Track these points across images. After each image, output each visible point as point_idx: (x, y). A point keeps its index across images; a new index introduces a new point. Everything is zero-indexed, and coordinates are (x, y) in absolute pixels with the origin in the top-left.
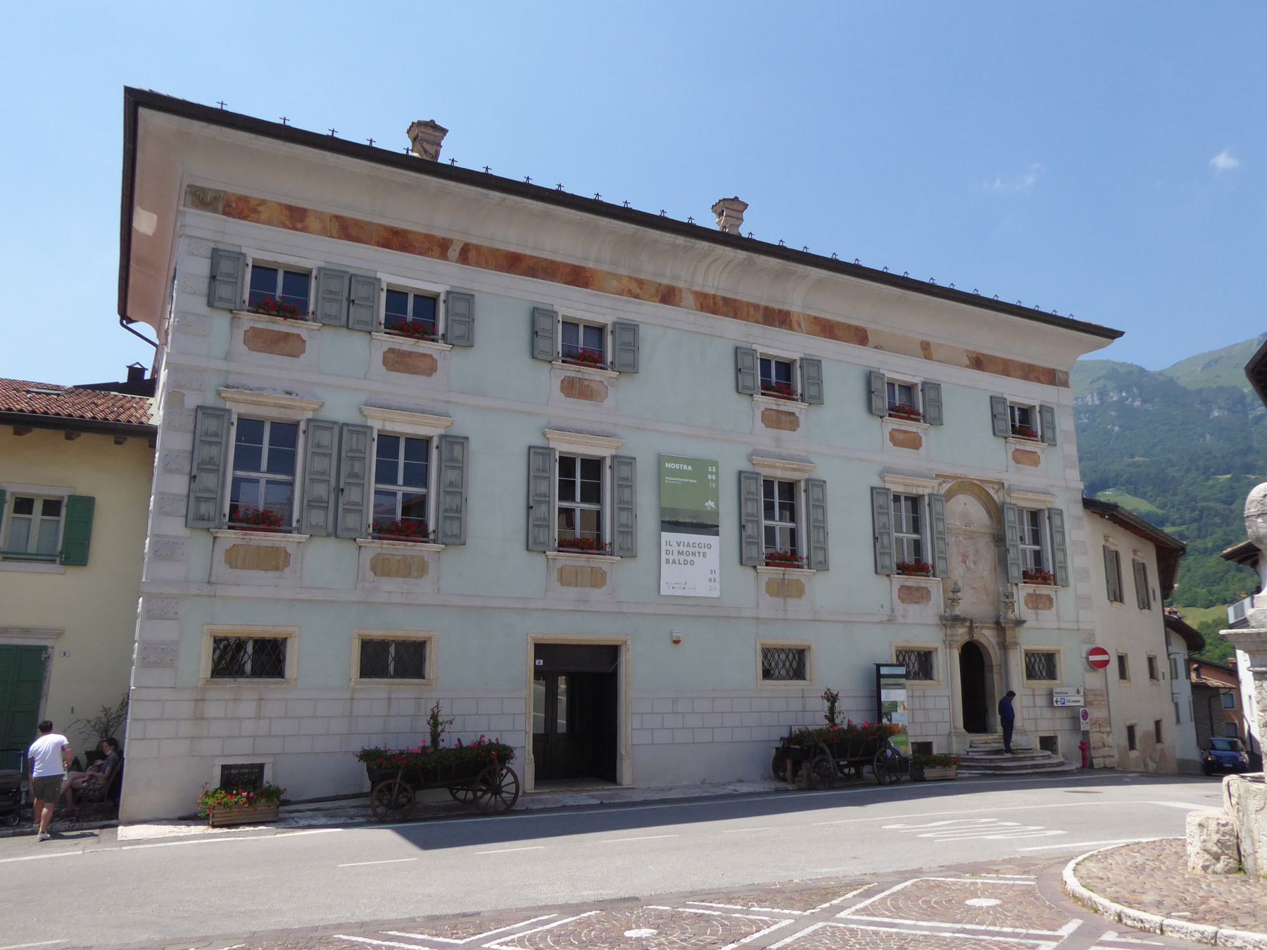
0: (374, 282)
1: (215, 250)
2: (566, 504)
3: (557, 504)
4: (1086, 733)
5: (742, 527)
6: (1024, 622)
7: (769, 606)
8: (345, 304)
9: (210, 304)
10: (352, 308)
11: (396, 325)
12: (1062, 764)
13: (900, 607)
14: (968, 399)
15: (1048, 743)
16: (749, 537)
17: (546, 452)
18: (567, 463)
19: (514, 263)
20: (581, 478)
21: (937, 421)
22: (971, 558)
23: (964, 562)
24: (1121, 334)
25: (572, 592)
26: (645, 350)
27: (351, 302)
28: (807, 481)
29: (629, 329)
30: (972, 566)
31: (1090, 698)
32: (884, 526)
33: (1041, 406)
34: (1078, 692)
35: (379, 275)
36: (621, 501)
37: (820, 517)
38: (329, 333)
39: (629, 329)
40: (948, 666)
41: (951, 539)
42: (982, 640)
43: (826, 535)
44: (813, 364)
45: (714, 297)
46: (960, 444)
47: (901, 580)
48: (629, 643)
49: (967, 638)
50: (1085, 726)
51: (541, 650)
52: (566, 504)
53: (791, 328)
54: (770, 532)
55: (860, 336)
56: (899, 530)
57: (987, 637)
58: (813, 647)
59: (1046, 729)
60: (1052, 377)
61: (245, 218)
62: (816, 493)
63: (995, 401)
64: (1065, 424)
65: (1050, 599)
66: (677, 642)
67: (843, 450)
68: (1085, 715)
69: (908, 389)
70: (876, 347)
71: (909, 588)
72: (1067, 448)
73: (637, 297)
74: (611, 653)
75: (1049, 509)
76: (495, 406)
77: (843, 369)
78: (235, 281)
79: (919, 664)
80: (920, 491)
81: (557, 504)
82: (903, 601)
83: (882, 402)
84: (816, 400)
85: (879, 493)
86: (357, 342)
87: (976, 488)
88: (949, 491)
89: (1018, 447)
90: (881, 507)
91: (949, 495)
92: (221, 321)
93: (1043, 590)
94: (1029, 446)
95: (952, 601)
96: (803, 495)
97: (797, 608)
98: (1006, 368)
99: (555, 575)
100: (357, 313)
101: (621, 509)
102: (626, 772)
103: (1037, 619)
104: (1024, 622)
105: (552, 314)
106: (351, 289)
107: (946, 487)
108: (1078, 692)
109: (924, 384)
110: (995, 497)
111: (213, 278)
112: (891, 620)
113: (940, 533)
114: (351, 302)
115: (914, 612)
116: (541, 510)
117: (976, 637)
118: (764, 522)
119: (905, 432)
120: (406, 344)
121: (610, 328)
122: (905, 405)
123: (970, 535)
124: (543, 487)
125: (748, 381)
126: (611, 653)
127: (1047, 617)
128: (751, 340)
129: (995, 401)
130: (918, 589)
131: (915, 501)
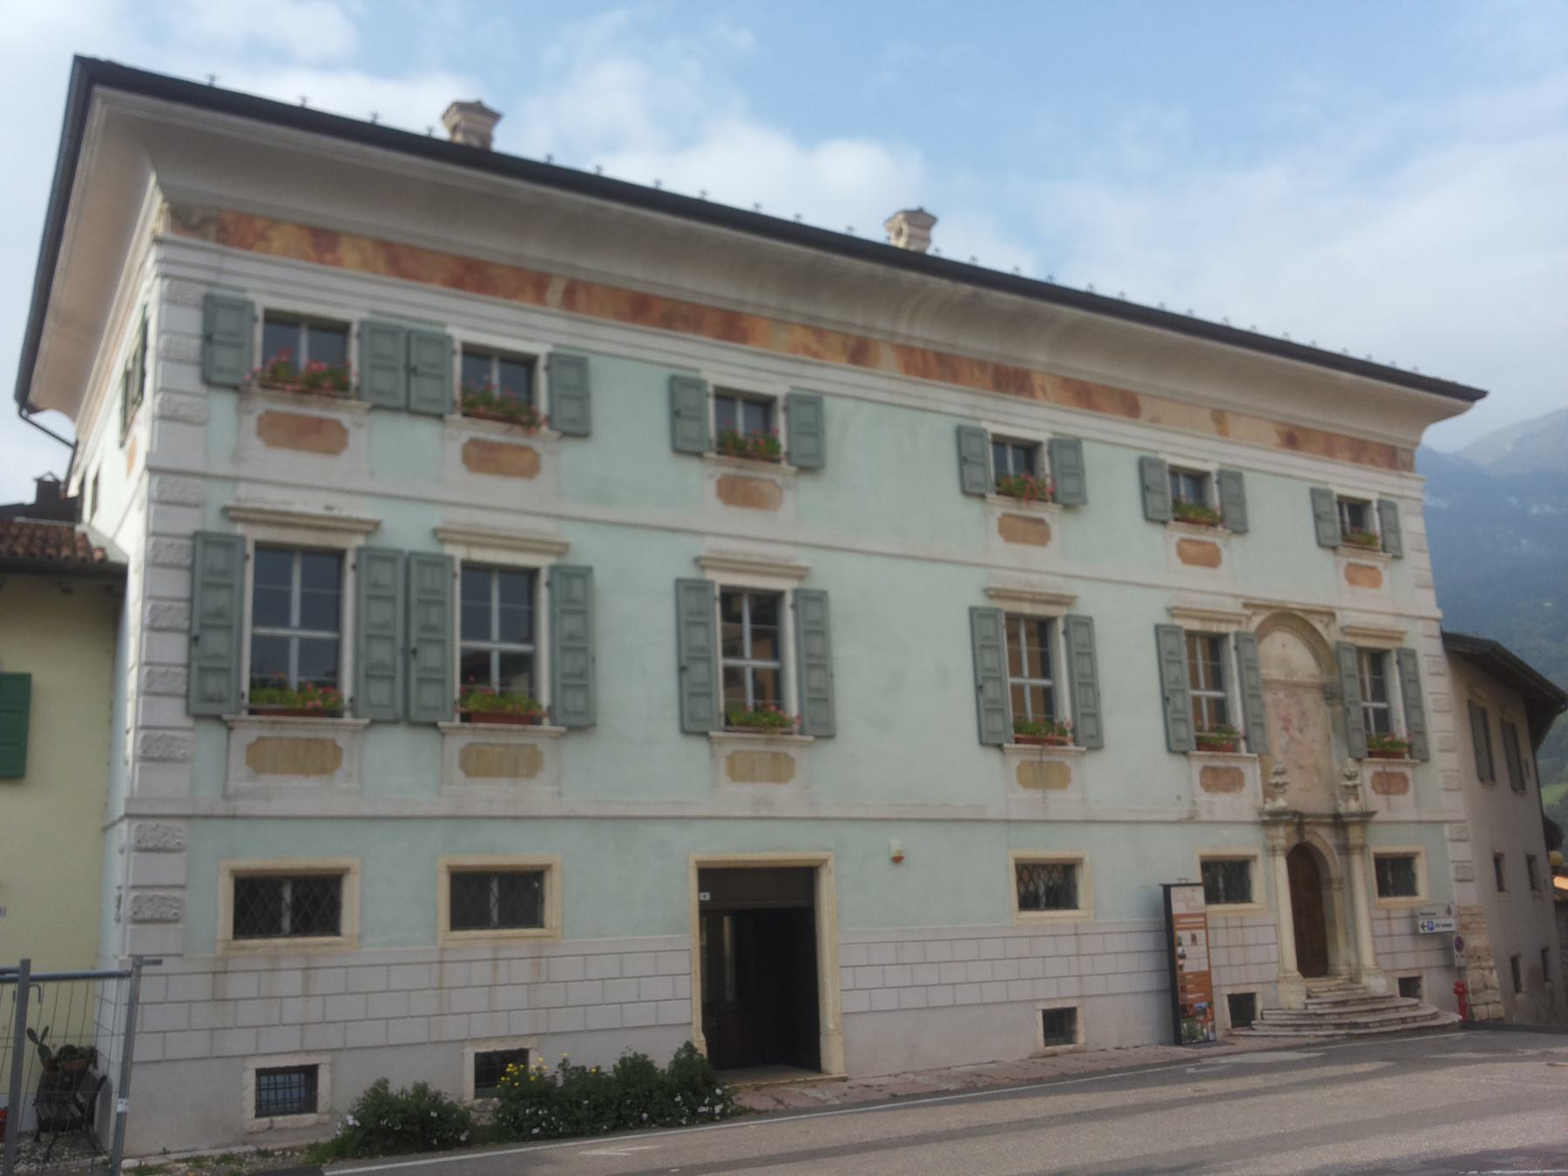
0: (443, 341)
1: (208, 299)
2: (732, 662)
3: (721, 662)
4: (1461, 970)
5: (979, 689)
6: (1373, 813)
7: (1024, 802)
8: (402, 374)
9: (207, 382)
10: (414, 382)
11: (475, 406)
12: (1435, 1016)
13: (1204, 798)
14: (1282, 492)
15: (1409, 986)
16: (990, 701)
17: (701, 587)
18: (730, 597)
19: (641, 309)
20: (753, 616)
21: (1240, 529)
22: (1296, 722)
23: (1286, 729)
24: (1472, 395)
25: (749, 790)
26: (832, 432)
27: (411, 371)
28: (1067, 618)
29: (809, 404)
30: (1298, 736)
31: (1466, 919)
32: (1177, 682)
33: (1380, 502)
34: (1449, 911)
35: (450, 330)
36: (810, 655)
37: (1088, 671)
38: (382, 421)
39: (809, 404)
40: (1272, 883)
41: (1268, 697)
42: (1316, 842)
43: (1097, 695)
44: (1070, 446)
45: (924, 352)
46: (1277, 557)
47: (1200, 760)
48: (831, 862)
49: (1295, 841)
50: (1459, 961)
51: (710, 876)
52: (732, 662)
53: (1032, 394)
54: (1017, 691)
55: (1129, 405)
56: (1195, 685)
57: (1324, 839)
58: (1087, 860)
59: (1408, 964)
60: (1394, 458)
61: (249, 247)
62: (1080, 635)
63: (1318, 495)
64: (1412, 526)
65: (1404, 779)
66: (897, 860)
67: (1119, 576)
68: (1460, 944)
69: (1198, 479)
70: (1152, 421)
71: (1214, 770)
72: (1417, 561)
73: (816, 355)
74: (804, 877)
75: (1399, 651)
76: (629, 518)
77: (1112, 454)
78: (239, 342)
79: (1226, 879)
80: (1223, 628)
81: (721, 662)
82: (1208, 788)
83: (1163, 502)
84: (1072, 502)
85: (1166, 633)
86: (423, 433)
87: (1287, 618)
88: (1262, 625)
89: (1352, 560)
90: (1170, 653)
91: (1263, 631)
92: (222, 405)
93: (1394, 767)
94: (1366, 560)
95: (1271, 790)
96: (1062, 640)
97: (1062, 802)
98: (1328, 445)
99: (723, 765)
100: (424, 388)
101: (810, 666)
102: (834, 1054)
103: (1389, 807)
104: (1373, 813)
105: (698, 385)
106: (411, 351)
107: (1257, 621)
108: (1449, 911)
109: (1221, 473)
110: (1324, 633)
111: (208, 338)
112: (1192, 819)
113: (1253, 688)
114: (411, 371)
115: (1223, 804)
116: (698, 672)
117: (1308, 838)
118: (1010, 680)
119: (1198, 543)
120: (492, 432)
121: (781, 403)
122: (1193, 504)
123: (1292, 687)
124: (699, 637)
125: (976, 474)
126: (804, 877)
127: (1402, 807)
128: (979, 414)
129: (1318, 495)
130: (1227, 770)
131: (1215, 643)
